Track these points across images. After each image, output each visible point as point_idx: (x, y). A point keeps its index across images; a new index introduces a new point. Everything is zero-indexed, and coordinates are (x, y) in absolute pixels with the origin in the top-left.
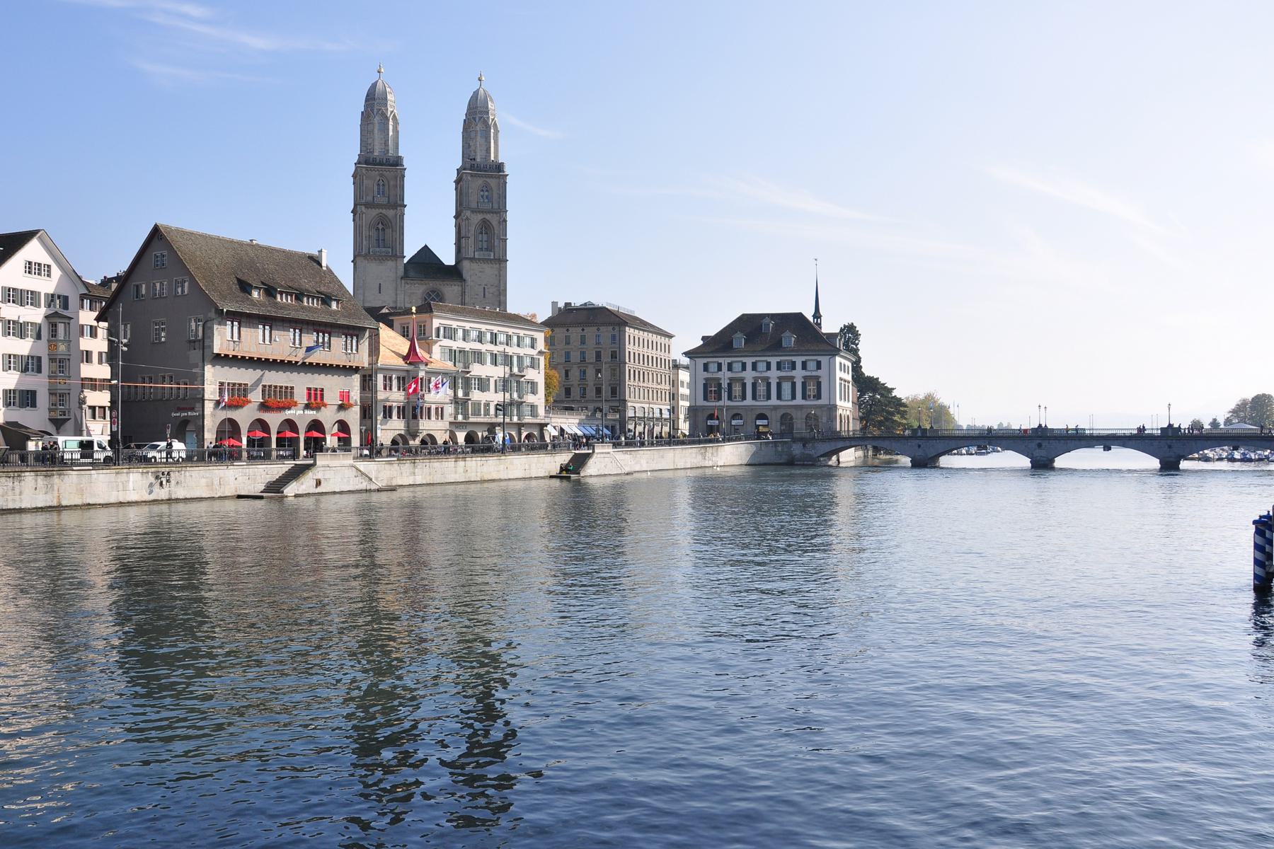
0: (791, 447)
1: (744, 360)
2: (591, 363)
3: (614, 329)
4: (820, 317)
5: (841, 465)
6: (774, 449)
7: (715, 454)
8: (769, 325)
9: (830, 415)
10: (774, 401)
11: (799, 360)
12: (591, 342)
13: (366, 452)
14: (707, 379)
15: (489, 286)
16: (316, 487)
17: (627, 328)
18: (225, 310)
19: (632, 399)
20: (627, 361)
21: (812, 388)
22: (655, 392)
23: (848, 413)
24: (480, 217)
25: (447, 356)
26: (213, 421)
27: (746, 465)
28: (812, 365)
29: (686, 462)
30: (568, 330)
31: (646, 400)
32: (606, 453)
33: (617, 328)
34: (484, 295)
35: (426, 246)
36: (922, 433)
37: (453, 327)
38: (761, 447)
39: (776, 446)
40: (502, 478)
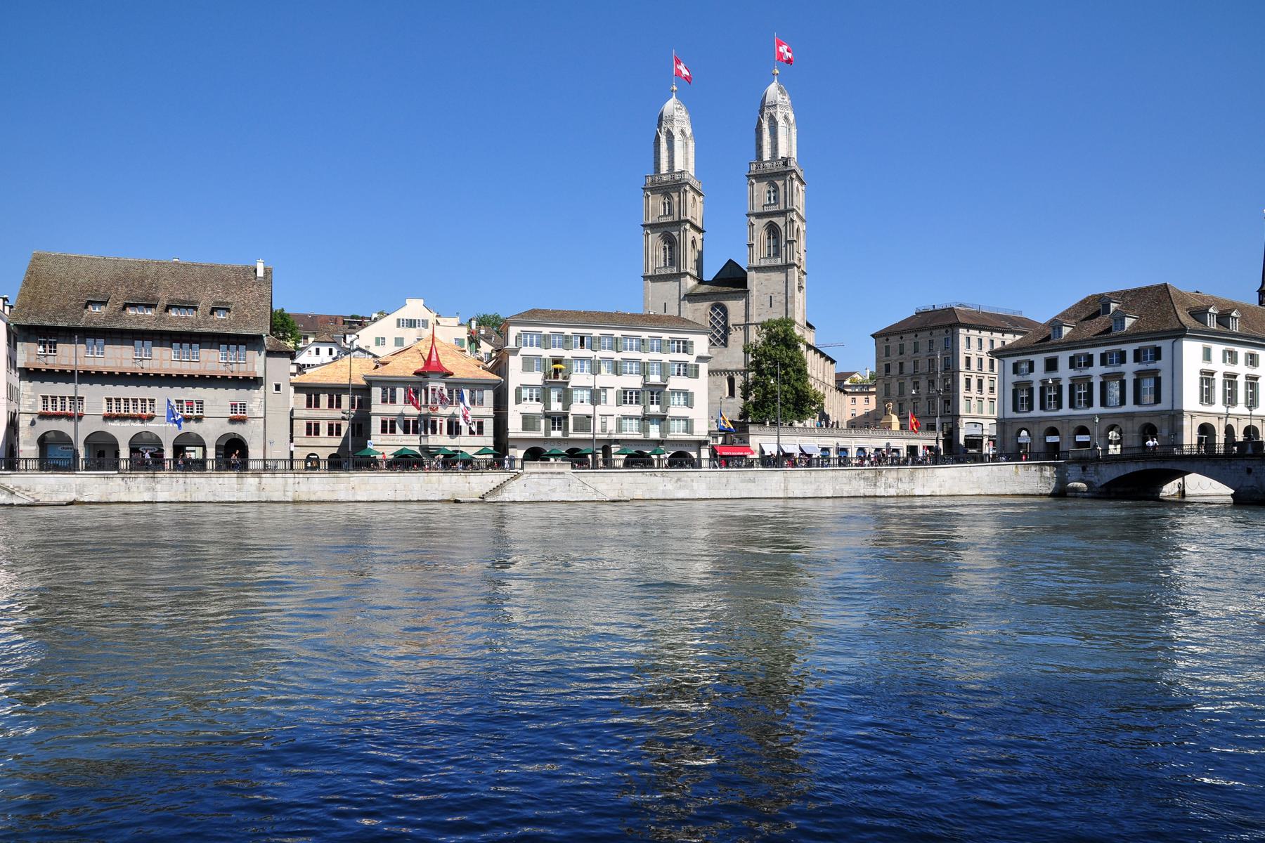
0: (1066, 472)
2: (924, 374)
3: (947, 332)
6: (1038, 474)
9: (1173, 424)
10: (1097, 408)
12: (924, 349)
15: (776, 294)
19: (974, 412)
20: (962, 366)
21: (1148, 384)
24: (766, 220)
26: (32, 434)
30: (902, 338)
32: (552, 473)
35: (730, 260)
36: (1254, 449)
38: (1017, 473)
39: (1041, 471)
40: (340, 499)
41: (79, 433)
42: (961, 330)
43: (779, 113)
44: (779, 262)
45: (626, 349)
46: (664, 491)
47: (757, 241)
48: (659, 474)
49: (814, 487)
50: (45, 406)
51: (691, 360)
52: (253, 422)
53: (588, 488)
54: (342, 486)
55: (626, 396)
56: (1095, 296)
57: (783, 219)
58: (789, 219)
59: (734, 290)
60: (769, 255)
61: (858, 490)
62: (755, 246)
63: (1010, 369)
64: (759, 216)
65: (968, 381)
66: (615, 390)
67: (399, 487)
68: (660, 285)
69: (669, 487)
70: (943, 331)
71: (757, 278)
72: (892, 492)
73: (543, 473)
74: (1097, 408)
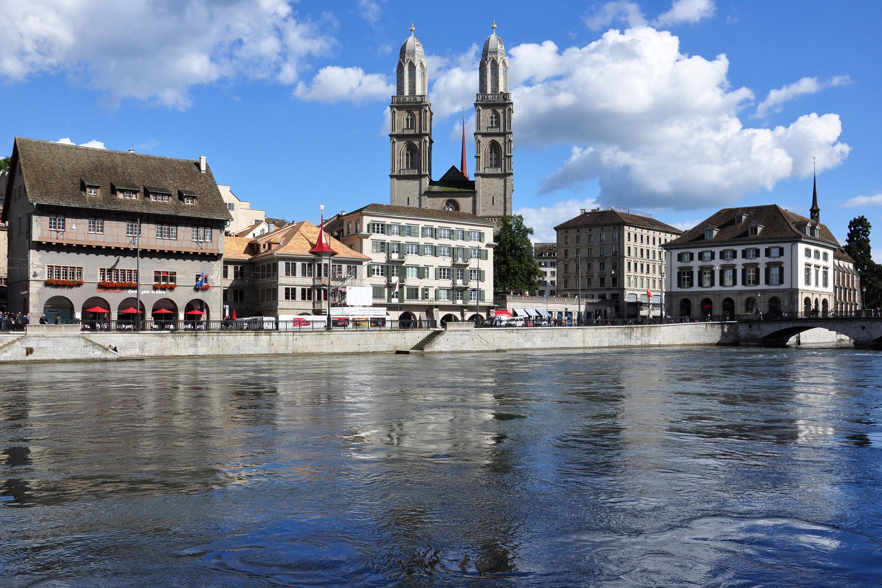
0: (738, 329)
1: (713, 249)
2: (596, 258)
4: (817, 211)
5: (801, 346)
7: (646, 334)
8: (741, 217)
9: (792, 298)
11: (762, 248)
13: (189, 326)
14: (680, 268)
16: (27, 354)
17: (626, 228)
18: (35, 204)
19: (632, 287)
20: (626, 254)
21: (775, 271)
22: (651, 281)
23: (827, 297)
24: (490, 139)
25: (379, 249)
27: (717, 345)
28: (775, 252)
29: (601, 341)
30: (578, 231)
31: (639, 287)
32: (463, 331)
33: (617, 227)
34: (493, 203)
37: (434, 227)
38: (706, 329)
41: (78, 297)
42: (626, 228)
43: (499, 58)
44: (499, 171)
45: (441, 237)
46: (518, 344)
47: (483, 154)
48: (515, 331)
49: (598, 339)
50: (157, 279)
51: (483, 246)
52: (213, 290)
53: (483, 341)
54: (325, 342)
55: (442, 273)
56: (727, 209)
57: (502, 138)
58: (507, 140)
59: (464, 190)
60: (491, 165)
61: (621, 341)
62: (481, 158)
63: (675, 257)
64: (484, 135)
65: (629, 263)
66: (434, 268)
67: (362, 342)
68: (403, 183)
69: (521, 340)
70: (612, 227)
71: (483, 182)
72: (639, 343)
73: (458, 331)
74: (762, 285)
